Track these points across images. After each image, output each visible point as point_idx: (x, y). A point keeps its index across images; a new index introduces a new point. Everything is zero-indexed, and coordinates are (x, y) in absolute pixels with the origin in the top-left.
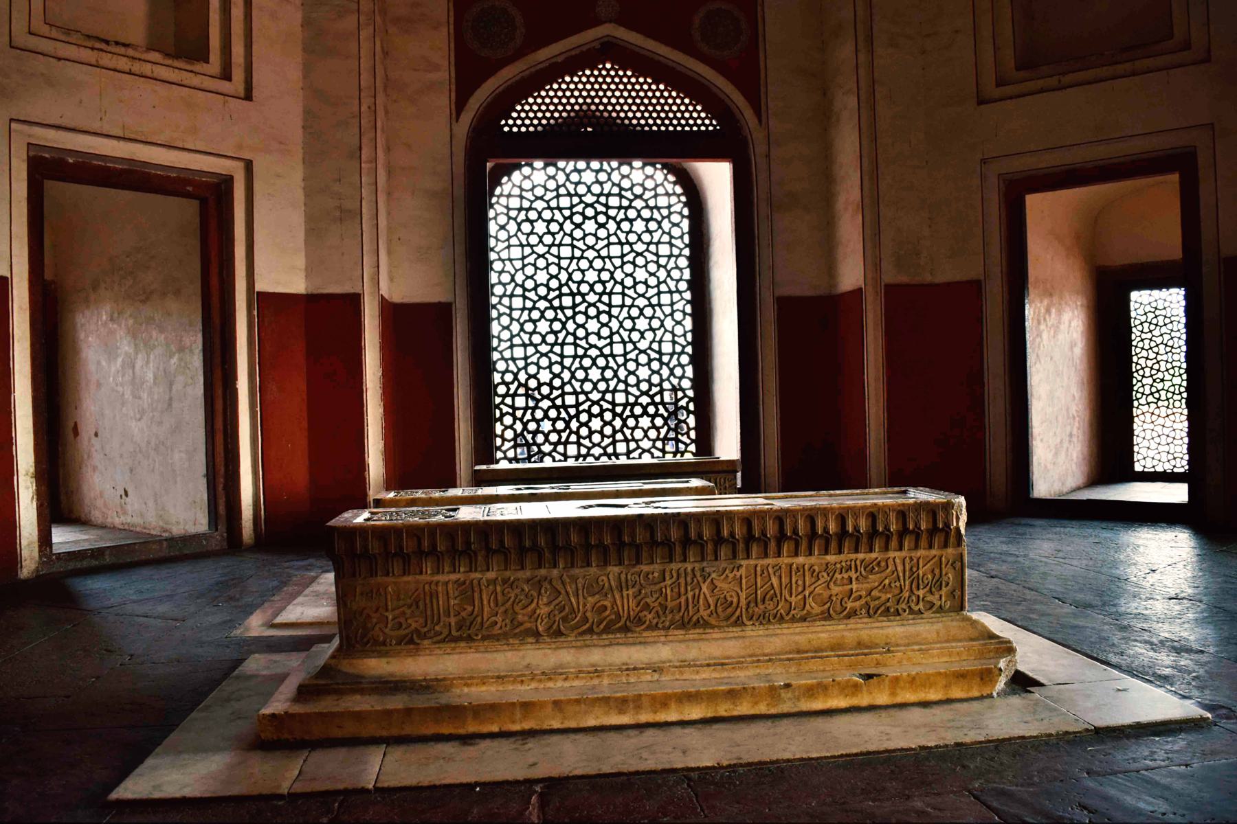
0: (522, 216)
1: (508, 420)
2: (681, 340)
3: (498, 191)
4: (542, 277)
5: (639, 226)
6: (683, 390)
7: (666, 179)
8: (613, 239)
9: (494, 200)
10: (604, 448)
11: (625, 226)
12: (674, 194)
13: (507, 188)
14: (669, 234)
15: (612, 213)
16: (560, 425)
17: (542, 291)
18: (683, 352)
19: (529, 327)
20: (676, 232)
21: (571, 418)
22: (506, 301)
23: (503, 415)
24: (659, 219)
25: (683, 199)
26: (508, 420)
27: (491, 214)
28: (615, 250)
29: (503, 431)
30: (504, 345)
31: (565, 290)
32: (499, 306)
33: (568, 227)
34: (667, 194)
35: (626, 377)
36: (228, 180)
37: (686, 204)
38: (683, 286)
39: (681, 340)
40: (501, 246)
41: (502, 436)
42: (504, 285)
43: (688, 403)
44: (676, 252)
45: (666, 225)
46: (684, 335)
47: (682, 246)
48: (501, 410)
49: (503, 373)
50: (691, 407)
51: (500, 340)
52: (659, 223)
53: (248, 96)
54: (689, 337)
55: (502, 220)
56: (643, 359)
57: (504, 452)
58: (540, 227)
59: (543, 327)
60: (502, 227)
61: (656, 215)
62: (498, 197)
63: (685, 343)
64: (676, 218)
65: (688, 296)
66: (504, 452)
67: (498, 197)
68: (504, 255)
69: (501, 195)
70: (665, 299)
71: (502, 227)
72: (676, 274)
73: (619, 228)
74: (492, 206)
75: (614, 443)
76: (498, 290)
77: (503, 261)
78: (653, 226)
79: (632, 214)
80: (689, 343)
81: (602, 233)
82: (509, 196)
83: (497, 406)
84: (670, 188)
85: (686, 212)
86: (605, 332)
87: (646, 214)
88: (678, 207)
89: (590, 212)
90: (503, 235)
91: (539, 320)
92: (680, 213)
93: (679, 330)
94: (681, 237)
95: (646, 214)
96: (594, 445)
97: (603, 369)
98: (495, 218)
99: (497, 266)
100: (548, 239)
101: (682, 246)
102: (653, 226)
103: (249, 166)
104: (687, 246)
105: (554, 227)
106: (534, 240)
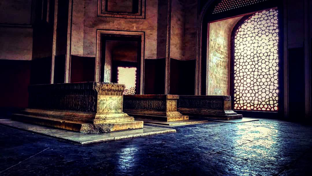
10: (266, 102)
16: (253, 95)
21: (256, 93)
29: (236, 96)
36: (141, 36)
41: (236, 97)
53: (145, 18)
57: (237, 102)
59: (249, 67)
67: (237, 32)
75: (269, 101)
83: (235, 89)
86: (267, 67)
90: (238, 43)
96: (263, 101)
103: (144, 32)
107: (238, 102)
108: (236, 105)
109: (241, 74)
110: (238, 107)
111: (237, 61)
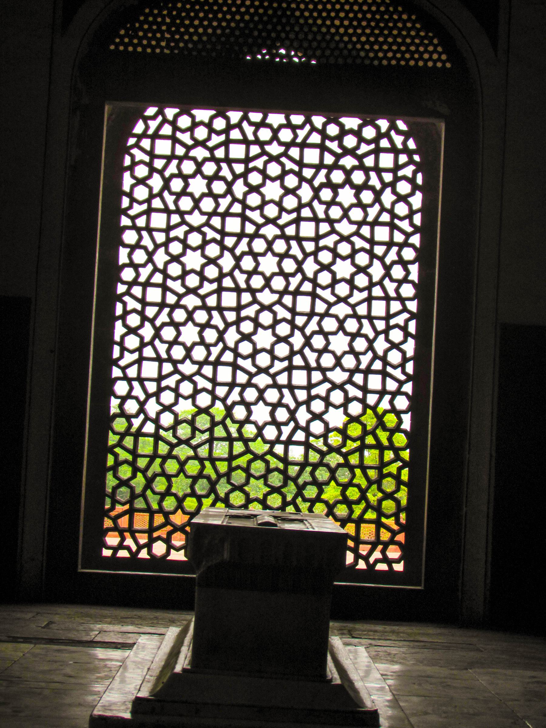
0: (172, 169)
1: (125, 472)
2: (397, 373)
3: (139, 128)
4: (193, 260)
5: (346, 196)
6: (397, 451)
7: (393, 126)
8: (306, 212)
9: (132, 141)
11: (326, 194)
12: (406, 150)
13: (153, 125)
14: (391, 212)
15: (308, 173)
17: (192, 281)
18: (398, 392)
19: (168, 333)
20: (401, 209)
22: (137, 291)
23: (118, 463)
24: (378, 186)
25: (417, 158)
26: (125, 472)
27: (127, 161)
28: (307, 229)
29: (115, 489)
30: (129, 358)
31: (227, 282)
32: (126, 298)
33: (239, 188)
34: (393, 150)
35: (308, 422)
37: (419, 168)
38: (408, 291)
39: (397, 373)
40: (137, 209)
42: (136, 267)
43: (400, 469)
44: (399, 238)
45: (388, 198)
46: (402, 365)
47: (410, 229)
48: (116, 455)
49: (124, 399)
50: (405, 475)
51: (123, 349)
52: (378, 195)
54: (410, 367)
55: (141, 171)
56: (337, 397)
57: (115, 520)
58: (198, 186)
60: (142, 182)
61: (374, 181)
62: (140, 137)
63: (403, 378)
64: (404, 188)
65: (413, 306)
66: (115, 520)
67: (140, 137)
68: (141, 222)
69: (144, 135)
70: (379, 308)
71: (142, 182)
72: (398, 272)
73: (316, 196)
74: (127, 150)
76: (128, 274)
77: (139, 230)
78: (367, 197)
79: (338, 177)
80: (409, 378)
81: (290, 202)
82: (156, 136)
83: (111, 450)
84: (398, 140)
85: (419, 179)
87: (358, 177)
88: (408, 171)
89: (274, 169)
90: (141, 193)
91: (184, 324)
92: (412, 181)
93: (395, 357)
94: (410, 217)
95: (358, 177)
97: (275, 407)
98: (131, 168)
99: (130, 237)
100: (208, 205)
101: (410, 229)
102: (367, 197)
104: (417, 230)
105: (219, 187)
106: (186, 203)
107: (124, 522)
108: (112, 540)
109: (150, 369)
110: (121, 546)
111: (128, 293)
